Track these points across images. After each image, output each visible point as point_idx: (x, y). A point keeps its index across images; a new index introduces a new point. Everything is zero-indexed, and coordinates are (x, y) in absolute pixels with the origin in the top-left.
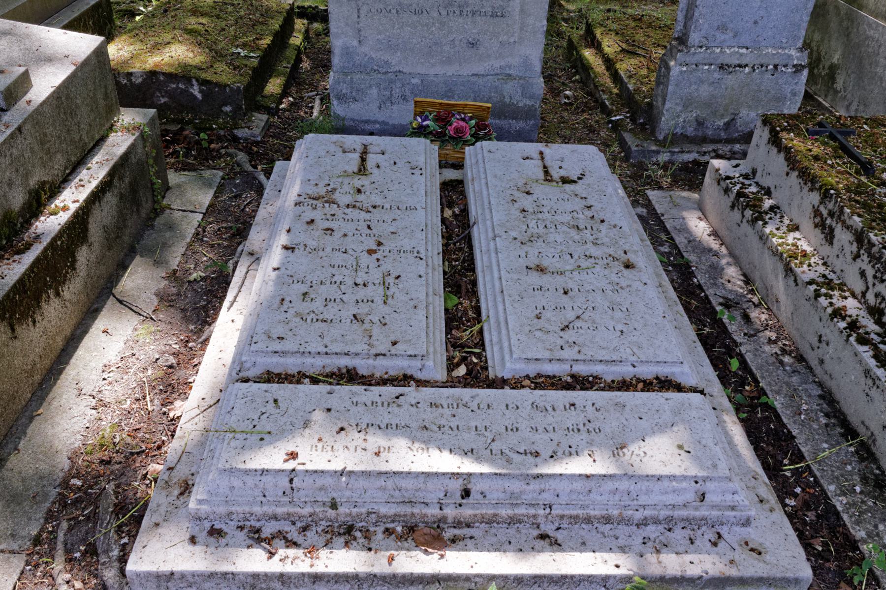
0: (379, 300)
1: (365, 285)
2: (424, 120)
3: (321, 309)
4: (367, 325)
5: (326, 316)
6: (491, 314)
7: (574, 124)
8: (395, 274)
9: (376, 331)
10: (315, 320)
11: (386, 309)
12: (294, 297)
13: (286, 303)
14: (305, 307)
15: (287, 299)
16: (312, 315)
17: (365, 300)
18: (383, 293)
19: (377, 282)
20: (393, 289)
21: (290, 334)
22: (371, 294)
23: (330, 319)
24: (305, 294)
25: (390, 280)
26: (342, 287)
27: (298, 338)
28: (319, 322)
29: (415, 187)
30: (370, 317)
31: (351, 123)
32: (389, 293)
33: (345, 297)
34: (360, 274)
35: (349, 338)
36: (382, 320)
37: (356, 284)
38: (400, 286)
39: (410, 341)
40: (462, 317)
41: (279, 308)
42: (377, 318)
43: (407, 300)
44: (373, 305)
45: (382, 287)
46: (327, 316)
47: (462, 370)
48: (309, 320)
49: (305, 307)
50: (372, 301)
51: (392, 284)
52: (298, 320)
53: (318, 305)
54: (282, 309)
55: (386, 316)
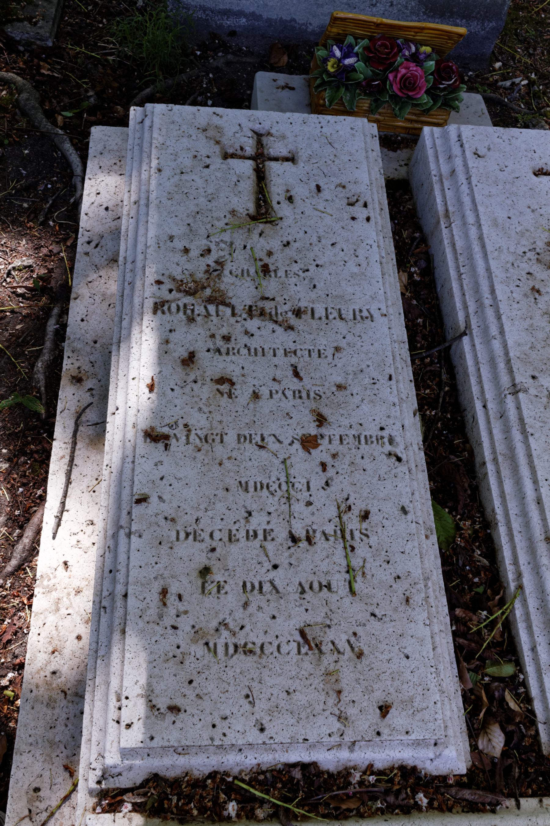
0: (339, 581)
1: (309, 539)
2: (346, 56)
3: (239, 613)
4: (328, 659)
5: (254, 637)
6: (527, 581)
7: (538, 13)
8: (358, 508)
9: (347, 676)
10: (231, 650)
11: (355, 610)
12: (185, 580)
13: (171, 599)
14: (204, 610)
15: (173, 589)
16: (225, 633)
17: (316, 586)
18: (344, 563)
19: (330, 529)
20: (362, 551)
21: (191, 693)
22: (324, 566)
23: (259, 643)
24: (205, 571)
25: (353, 523)
26: (270, 546)
27: (206, 704)
28: (240, 656)
29: (360, 252)
30: (331, 635)
31: (200, 14)
32: (356, 563)
33: (278, 576)
34: (298, 507)
35: (300, 698)
36: (353, 640)
37: (294, 540)
38: (373, 540)
39: (412, 700)
40: (464, 565)
41: (161, 617)
42: (344, 637)
43: (391, 581)
44: (334, 598)
45: (340, 545)
46: (252, 637)
47: (496, 741)
48: (221, 650)
49: (204, 610)
50: (329, 587)
51: (357, 534)
52: (199, 650)
53: (232, 598)
54: (168, 621)
55: (360, 631)
